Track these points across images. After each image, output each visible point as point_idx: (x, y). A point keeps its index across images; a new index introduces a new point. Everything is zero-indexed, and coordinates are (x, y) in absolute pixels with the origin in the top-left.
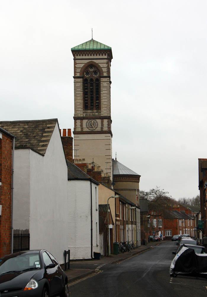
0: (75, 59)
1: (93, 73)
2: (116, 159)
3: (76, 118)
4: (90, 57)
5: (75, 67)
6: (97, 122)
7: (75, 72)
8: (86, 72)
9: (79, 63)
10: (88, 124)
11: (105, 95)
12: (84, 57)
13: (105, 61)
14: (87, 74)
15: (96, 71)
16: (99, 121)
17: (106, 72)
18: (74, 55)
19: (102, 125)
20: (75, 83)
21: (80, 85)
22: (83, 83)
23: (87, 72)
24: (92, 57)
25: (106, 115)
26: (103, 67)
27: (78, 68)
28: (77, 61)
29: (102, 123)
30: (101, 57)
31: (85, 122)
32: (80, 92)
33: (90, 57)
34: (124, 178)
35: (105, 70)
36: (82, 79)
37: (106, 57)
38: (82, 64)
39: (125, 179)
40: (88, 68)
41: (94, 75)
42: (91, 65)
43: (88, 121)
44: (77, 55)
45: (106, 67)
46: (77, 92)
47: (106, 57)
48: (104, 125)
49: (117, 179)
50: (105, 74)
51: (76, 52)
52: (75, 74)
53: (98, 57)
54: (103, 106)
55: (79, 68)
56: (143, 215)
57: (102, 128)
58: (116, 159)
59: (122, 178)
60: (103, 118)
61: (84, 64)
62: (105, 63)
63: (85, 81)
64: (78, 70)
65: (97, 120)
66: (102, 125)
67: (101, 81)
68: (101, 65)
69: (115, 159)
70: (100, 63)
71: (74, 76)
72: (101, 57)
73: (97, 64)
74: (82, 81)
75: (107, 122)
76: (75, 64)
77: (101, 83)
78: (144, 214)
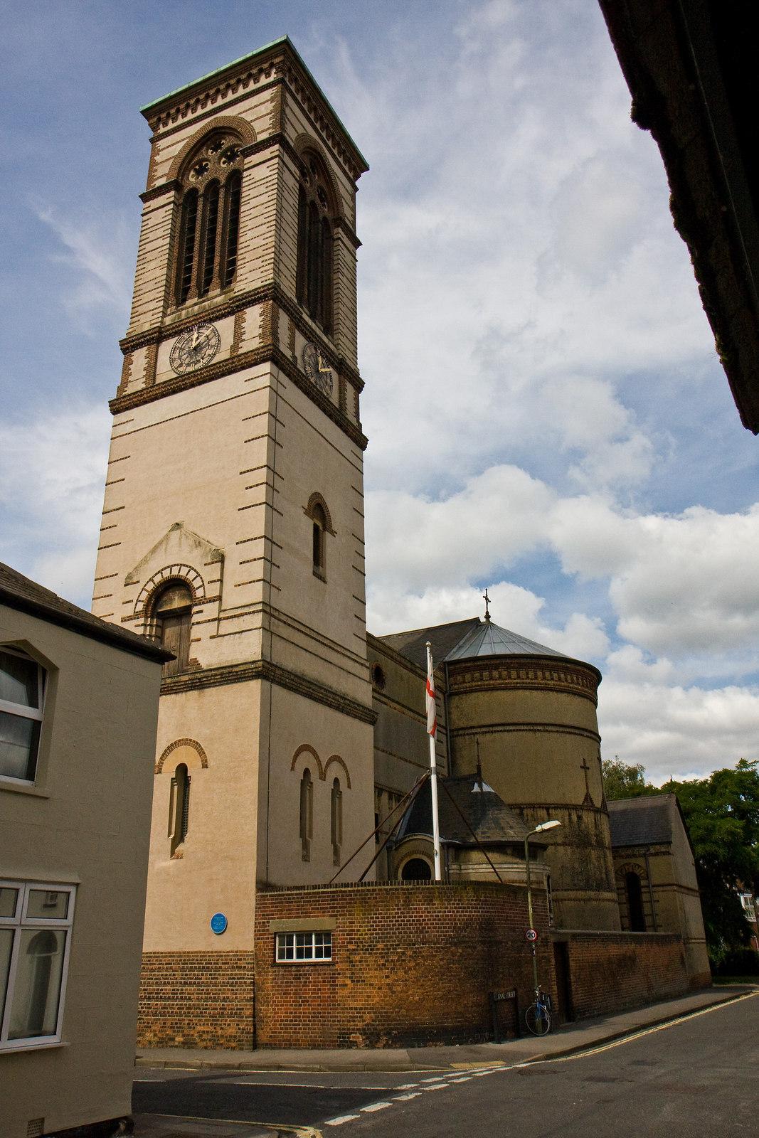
1: (224, 159)
2: (488, 617)
4: (210, 107)
6: (215, 331)
8: (197, 167)
9: (167, 147)
10: (176, 355)
11: (254, 212)
16: (225, 326)
17: (269, 129)
18: (154, 128)
19: (238, 335)
23: (200, 165)
26: (254, 120)
28: (162, 143)
30: (252, 86)
34: (495, 674)
38: (175, 146)
39: (500, 678)
40: (204, 150)
41: (225, 166)
42: (212, 138)
47: (273, 77)
48: (244, 333)
49: (464, 682)
54: (249, 256)
56: (651, 860)
57: (235, 347)
58: (488, 617)
59: (486, 674)
62: (267, 101)
63: (187, 203)
65: (218, 325)
66: (238, 335)
68: (248, 117)
69: (483, 620)
70: (241, 113)
72: (252, 86)
73: (236, 119)
75: (261, 315)
78: (656, 854)
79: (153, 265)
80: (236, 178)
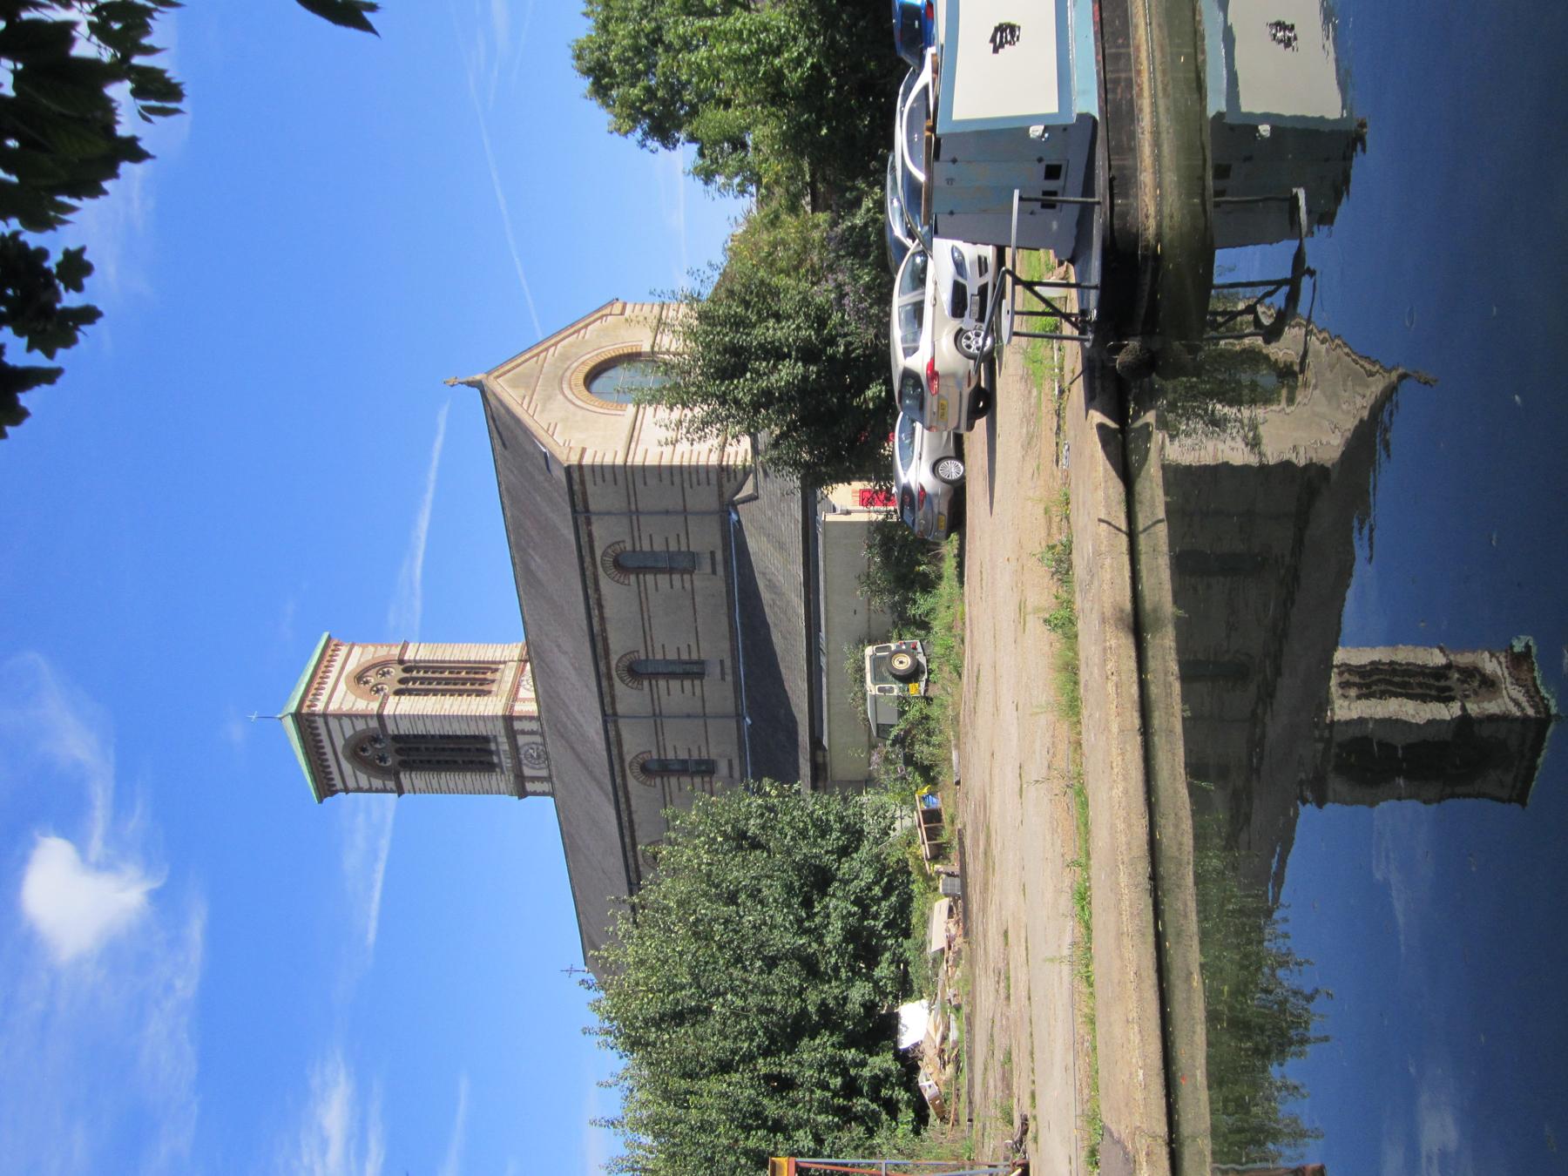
0: (347, 790)
3: (522, 793)
5: (370, 790)
6: (524, 745)
7: (385, 790)
12: (334, 769)
13: (333, 724)
14: (382, 759)
15: (370, 742)
16: (521, 740)
18: (336, 792)
20: (417, 790)
21: (419, 779)
22: (411, 771)
24: (328, 749)
25: (500, 725)
27: (370, 784)
28: (351, 784)
29: (523, 732)
31: (527, 772)
32: (441, 782)
33: (330, 756)
35: (360, 725)
36: (402, 775)
37: (320, 722)
43: (527, 766)
44: (334, 785)
45: (352, 723)
46: (444, 787)
50: (374, 724)
51: (325, 787)
52: (392, 791)
53: (324, 737)
55: (369, 781)
60: (512, 734)
61: (358, 773)
63: (410, 766)
64: (377, 783)
67: (396, 733)
68: (349, 732)
70: (344, 735)
71: (396, 795)
74: (408, 773)
76: (359, 790)
77: (402, 732)
79: (460, 783)
80: (397, 738)
